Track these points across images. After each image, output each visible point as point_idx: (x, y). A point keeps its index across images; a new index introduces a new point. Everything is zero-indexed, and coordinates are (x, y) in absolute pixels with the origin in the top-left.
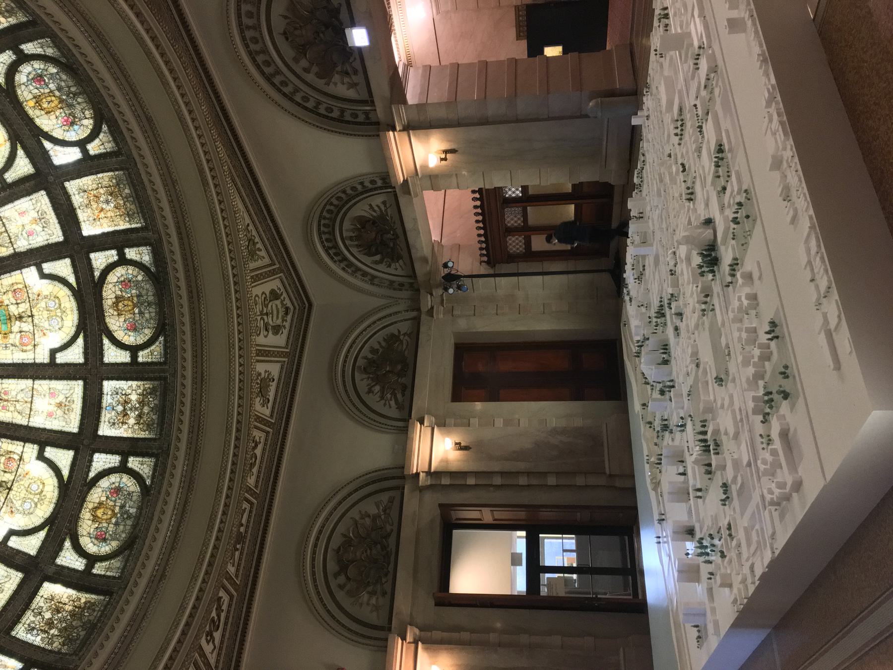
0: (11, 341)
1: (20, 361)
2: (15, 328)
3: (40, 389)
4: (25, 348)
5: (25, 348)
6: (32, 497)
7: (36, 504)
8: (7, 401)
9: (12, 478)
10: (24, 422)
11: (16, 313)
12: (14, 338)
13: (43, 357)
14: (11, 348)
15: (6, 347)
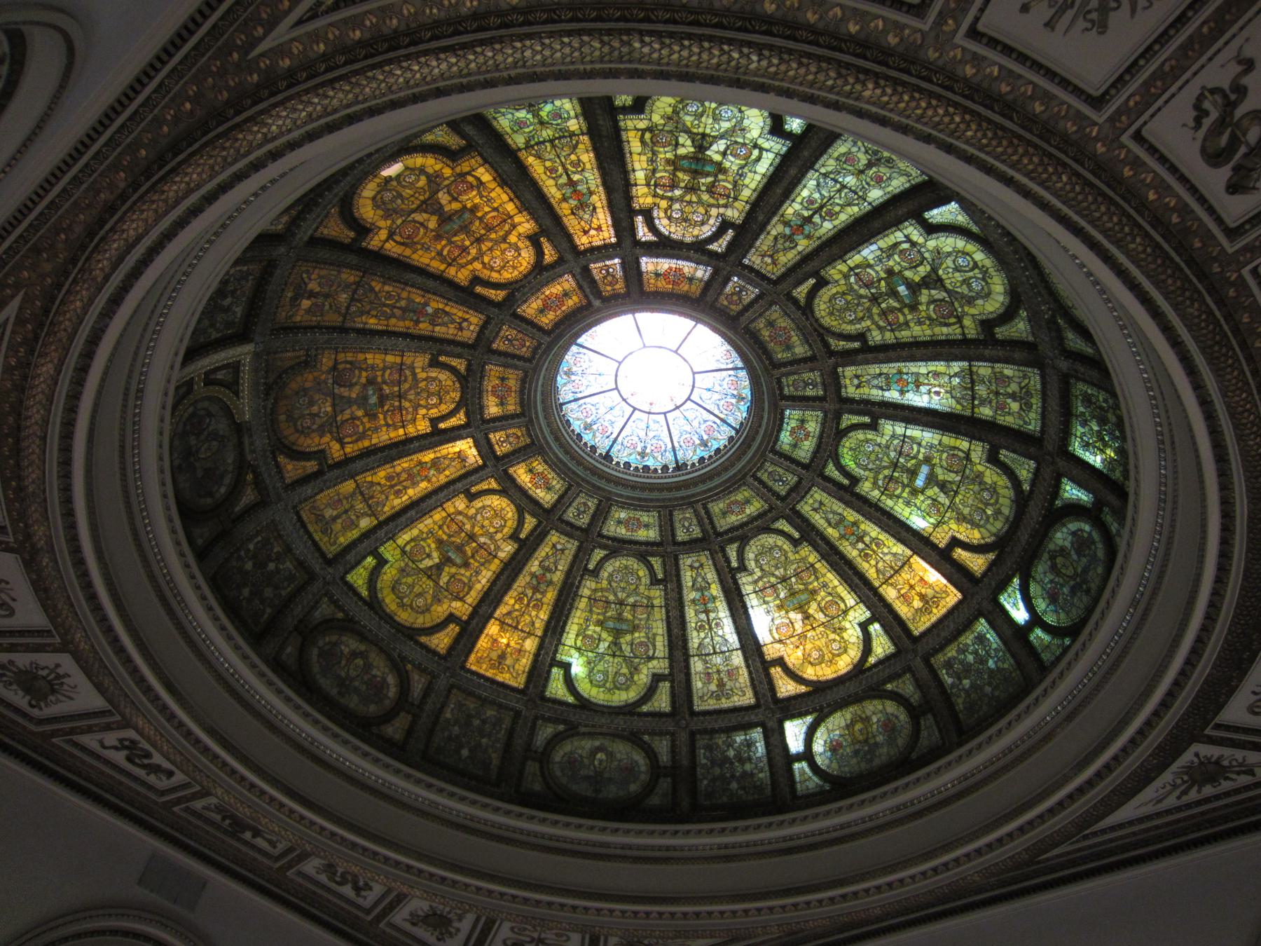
0: (735, 168)
1: (772, 169)
2: (717, 158)
3: (830, 169)
4: (753, 157)
5: (753, 157)
6: (971, 274)
7: (984, 279)
8: (822, 207)
9: (928, 268)
10: (866, 207)
11: (692, 150)
12: (732, 163)
13: (776, 146)
14: (746, 170)
15: (741, 175)
